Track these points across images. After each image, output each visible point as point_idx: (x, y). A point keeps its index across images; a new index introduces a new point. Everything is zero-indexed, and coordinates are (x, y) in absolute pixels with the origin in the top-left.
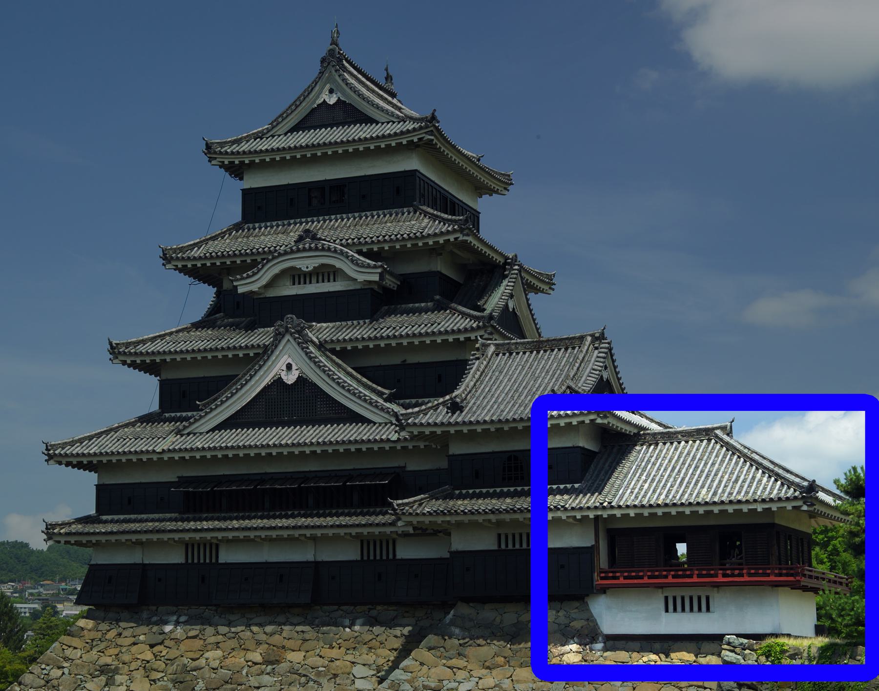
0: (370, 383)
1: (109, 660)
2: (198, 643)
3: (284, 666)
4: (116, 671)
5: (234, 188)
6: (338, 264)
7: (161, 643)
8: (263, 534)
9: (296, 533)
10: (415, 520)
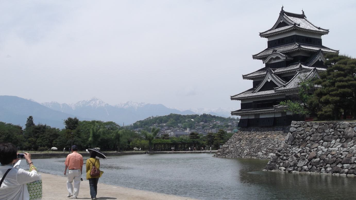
0: (282, 81)
1: (241, 138)
2: (256, 134)
3: (267, 138)
4: (242, 140)
5: (266, 40)
6: (280, 56)
7: (250, 134)
8: (264, 112)
9: (269, 112)
10: (278, 109)
